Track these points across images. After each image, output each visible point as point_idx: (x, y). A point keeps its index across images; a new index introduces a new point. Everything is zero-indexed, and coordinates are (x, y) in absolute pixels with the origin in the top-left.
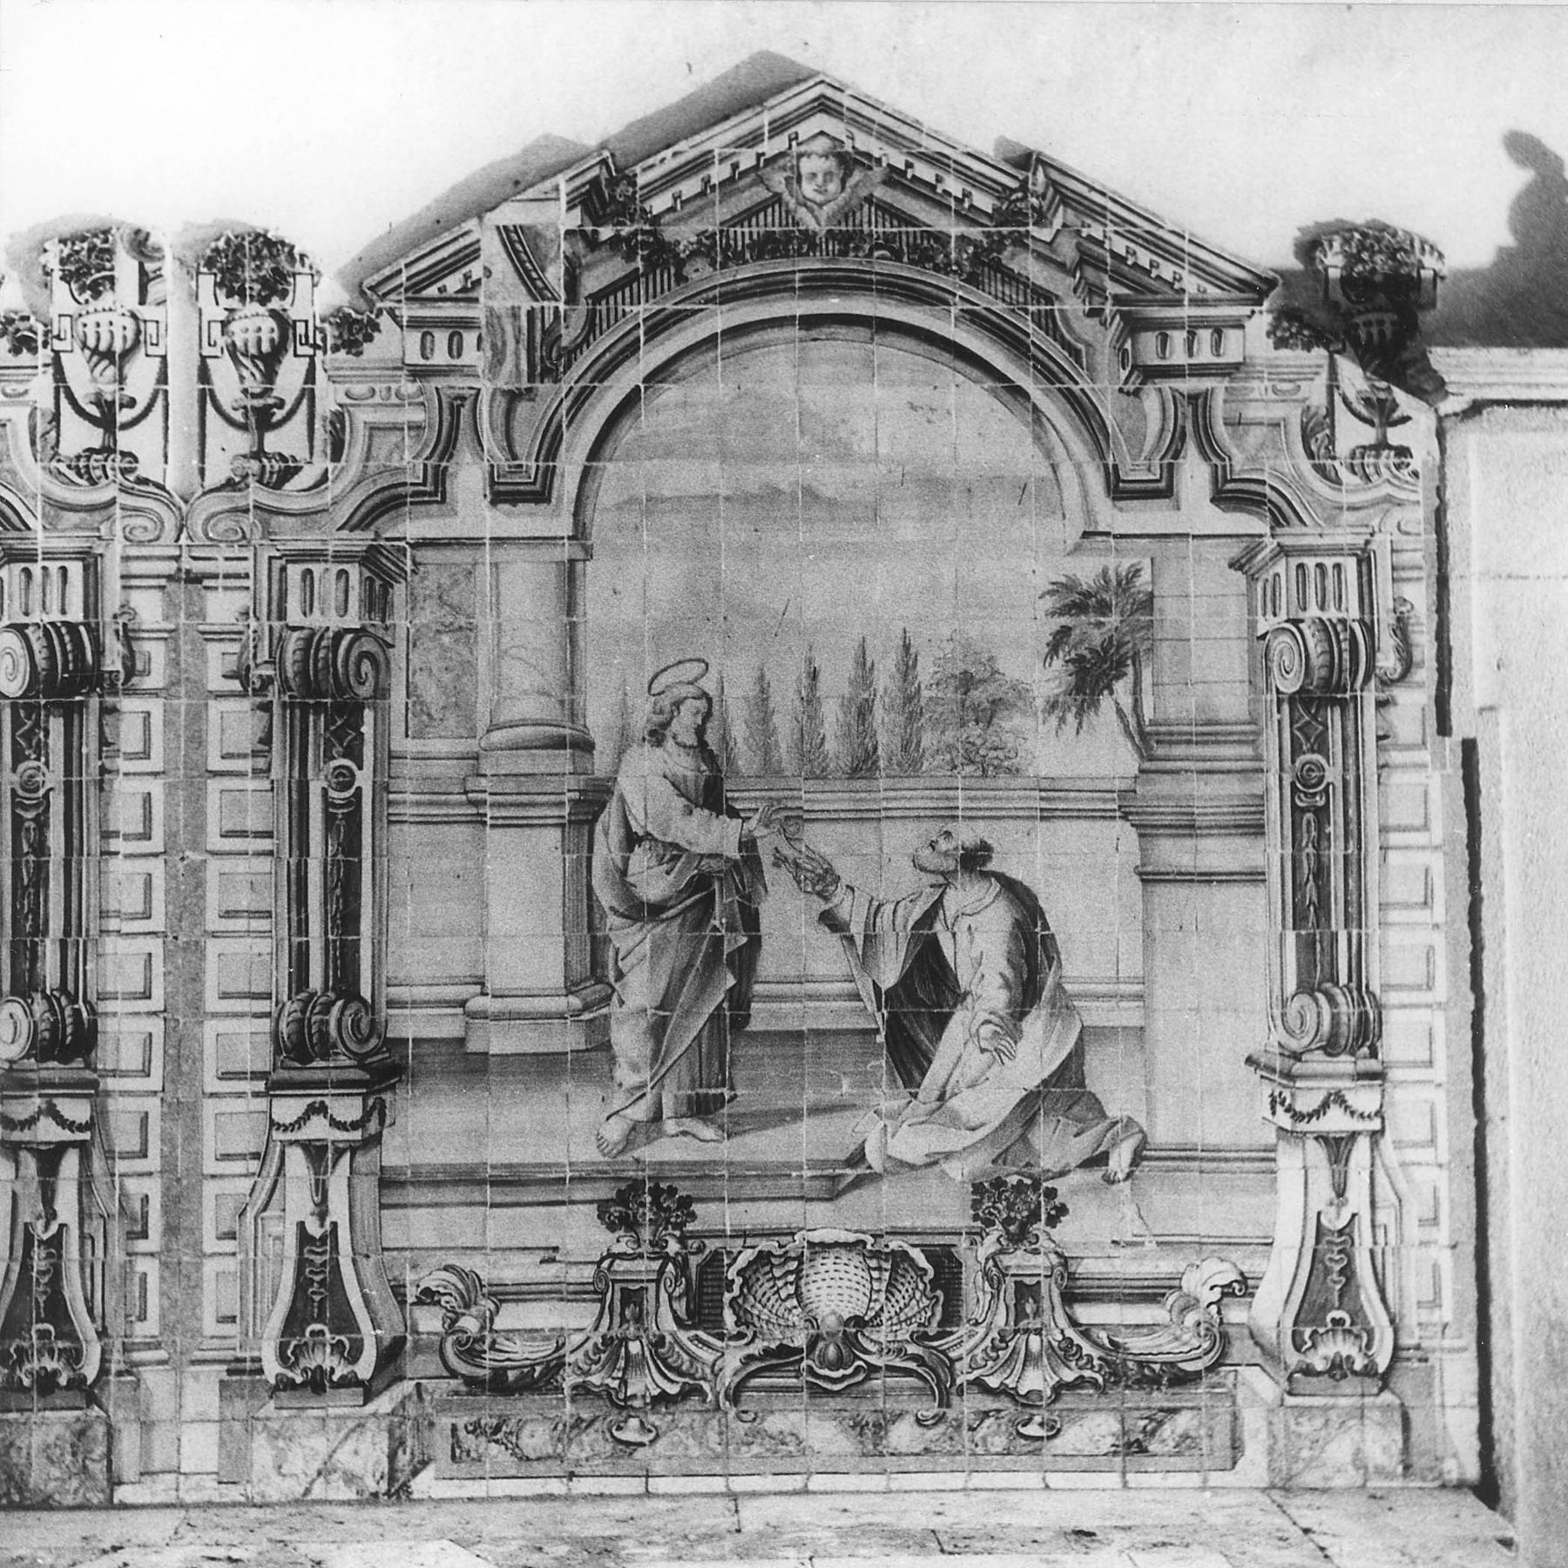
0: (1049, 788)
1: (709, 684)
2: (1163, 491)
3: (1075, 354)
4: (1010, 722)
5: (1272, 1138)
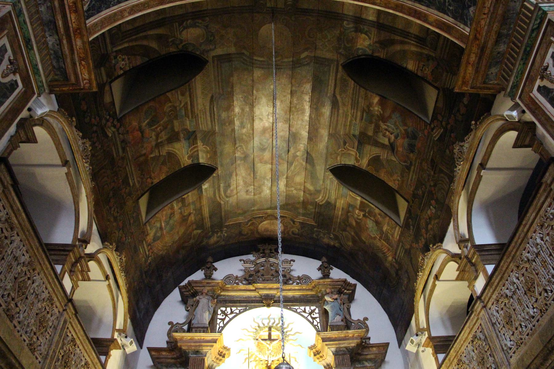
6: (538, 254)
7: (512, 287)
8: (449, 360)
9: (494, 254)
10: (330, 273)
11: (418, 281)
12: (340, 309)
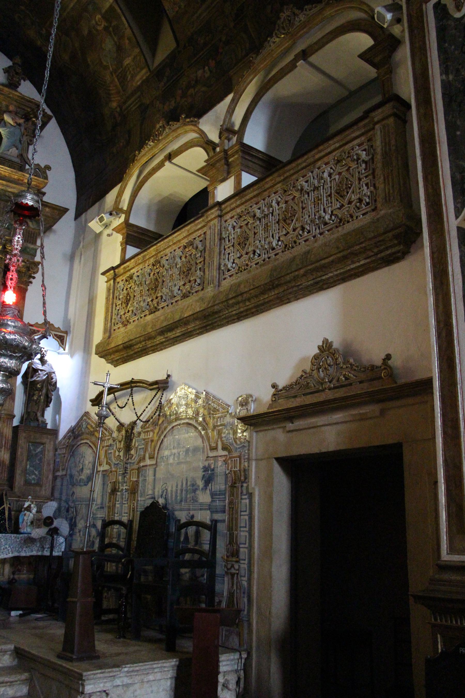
0: (201, 504)
1: (167, 487)
2: (216, 448)
3: (207, 424)
4: (198, 492)
5: (224, 573)
6: (316, 188)
7: (266, 210)
8: (144, 257)
9: (257, 164)
10: (20, 84)
11: (143, 152)
12: (20, 141)
